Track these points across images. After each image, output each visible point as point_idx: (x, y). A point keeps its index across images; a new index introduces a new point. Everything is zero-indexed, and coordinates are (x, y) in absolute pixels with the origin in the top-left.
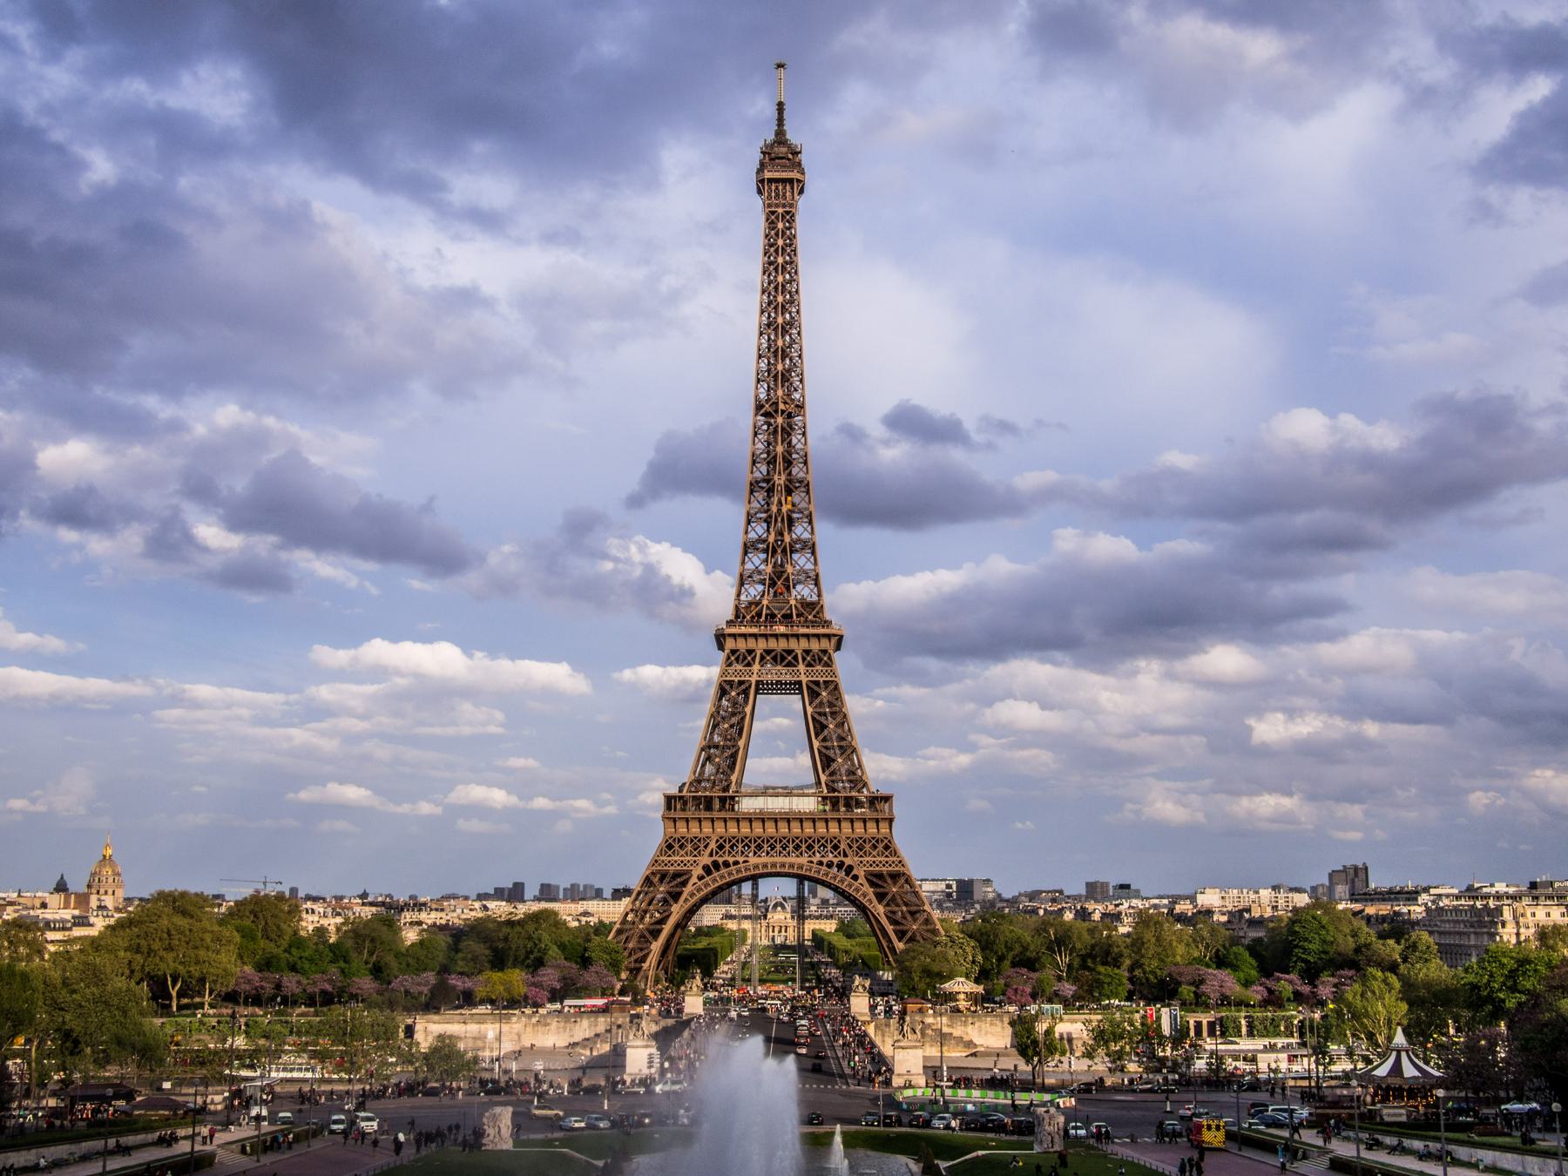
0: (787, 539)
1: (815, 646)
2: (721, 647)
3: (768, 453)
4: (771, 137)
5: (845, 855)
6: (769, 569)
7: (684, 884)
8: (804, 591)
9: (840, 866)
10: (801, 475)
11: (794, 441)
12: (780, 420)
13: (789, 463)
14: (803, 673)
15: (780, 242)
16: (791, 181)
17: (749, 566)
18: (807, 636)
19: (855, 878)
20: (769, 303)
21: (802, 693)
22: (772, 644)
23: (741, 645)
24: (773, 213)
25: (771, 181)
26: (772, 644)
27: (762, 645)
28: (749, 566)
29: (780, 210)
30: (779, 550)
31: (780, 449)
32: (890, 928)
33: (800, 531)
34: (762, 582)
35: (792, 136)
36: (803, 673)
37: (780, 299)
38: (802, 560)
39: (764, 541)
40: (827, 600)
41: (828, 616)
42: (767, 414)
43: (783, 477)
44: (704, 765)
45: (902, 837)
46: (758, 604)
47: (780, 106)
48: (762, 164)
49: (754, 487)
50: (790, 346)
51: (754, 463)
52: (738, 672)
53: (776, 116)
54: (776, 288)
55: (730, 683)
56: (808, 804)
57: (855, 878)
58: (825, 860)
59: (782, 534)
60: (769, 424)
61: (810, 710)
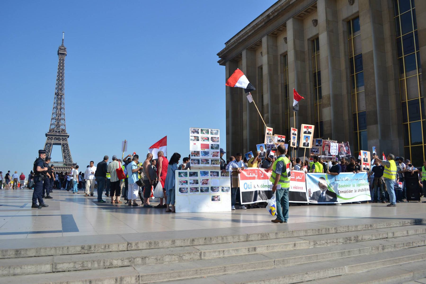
0: (60, 118)
1: (64, 137)
2: (46, 136)
4: (61, 45)
6: (56, 123)
8: (62, 127)
12: (60, 96)
13: (61, 104)
14: (61, 142)
16: (64, 54)
18: (63, 136)
23: (50, 137)
25: (60, 53)
27: (54, 137)
30: (58, 120)
31: (59, 102)
33: (62, 116)
36: (61, 142)
40: (66, 129)
41: (67, 132)
52: (50, 141)
55: (48, 143)
56: (61, 165)
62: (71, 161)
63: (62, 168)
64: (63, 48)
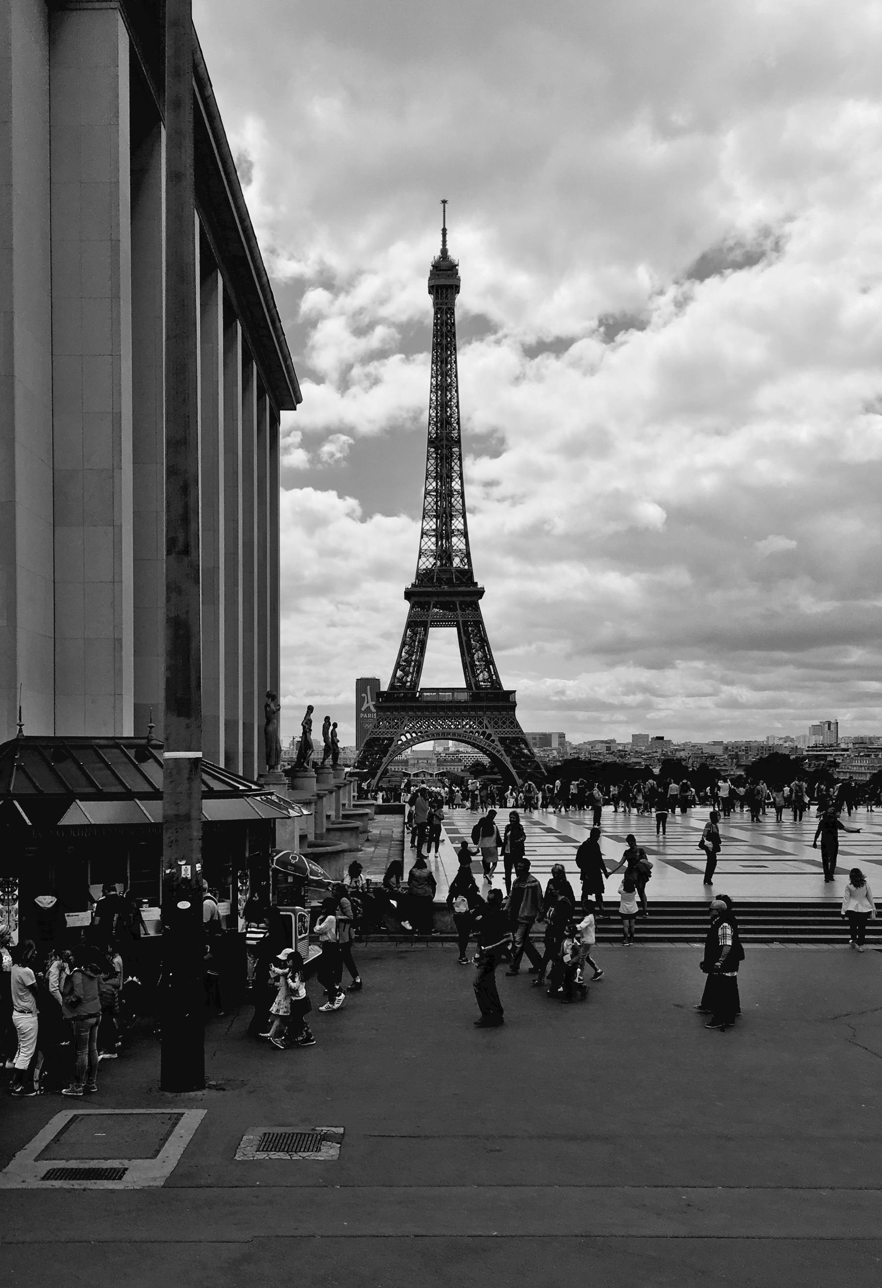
0: (449, 531)
1: (468, 599)
3: (437, 472)
4: (438, 254)
5: (487, 728)
7: (389, 745)
9: (484, 733)
11: (453, 464)
12: (445, 451)
15: (444, 330)
16: (451, 287)
19: (493, 741)
20: (437, 370)
21: (458, 626)
22: (441, 599)
24: (439, 309)
26: (441, 599)
28: (426, 547)
29: (444, 307)
31: (445, 471)
32: (513, 771)
33: (457, 524)
35: (453, 254)
37: (444, 370)
38: (457, 542)
42: (437, 449)
45: (520, 715)
46: (431, 570)
47: (444, 231)
49: (427, 493)
50: (450, 400)
56: (464, 697)
57: (493, 741)
58: (474, 731)
59: (445, 524)
60: (437, 454)
61: (464, 639)
62: (496, 683)
63: (466, 708)
64: (444, 264)
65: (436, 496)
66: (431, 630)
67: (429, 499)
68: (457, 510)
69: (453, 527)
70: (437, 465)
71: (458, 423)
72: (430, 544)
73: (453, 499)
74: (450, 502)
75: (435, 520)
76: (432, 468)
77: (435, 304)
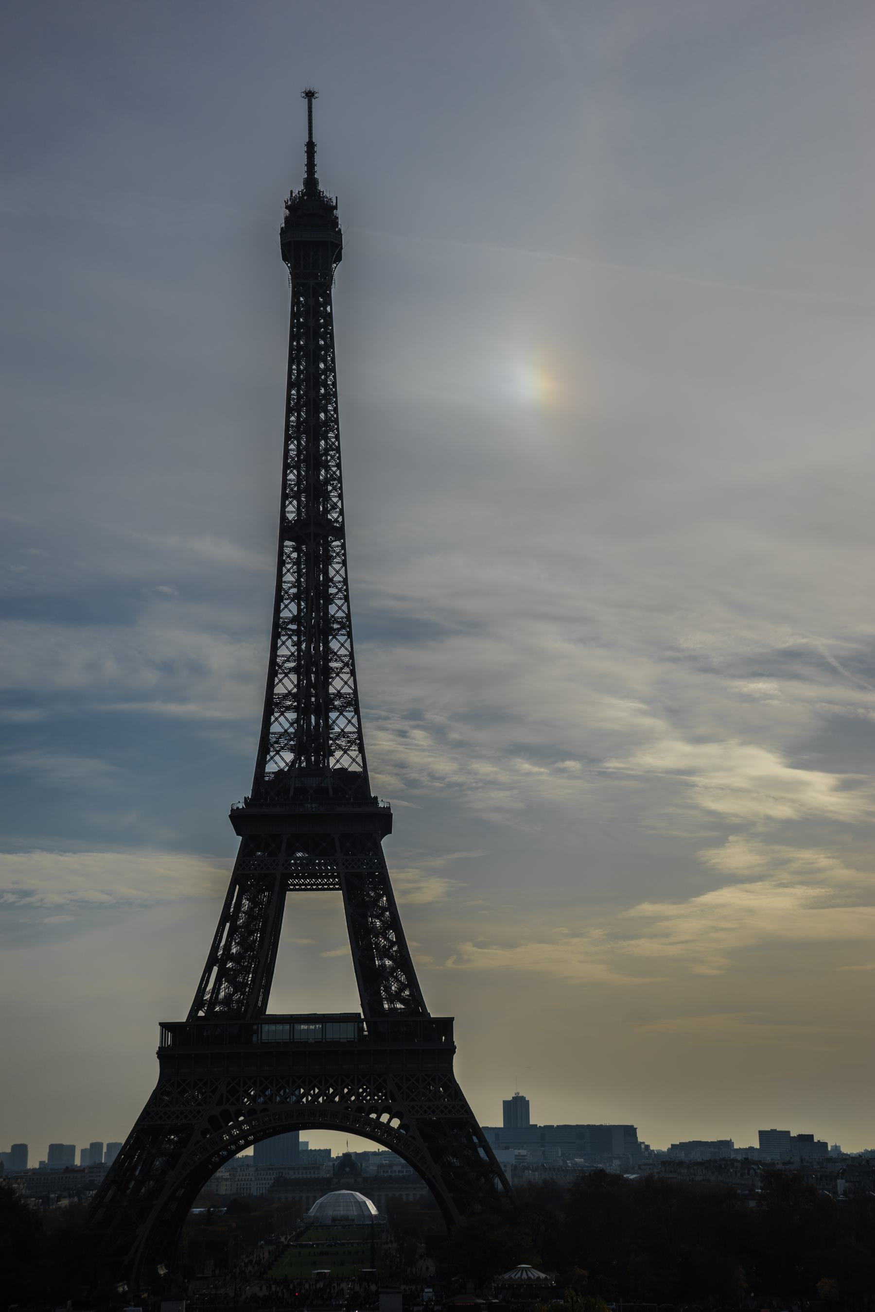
10: (340, 614)
11: (332, 573)
17: (275, 728)
33: (337, 685)
34: (292, 750)
38: (341, 723)
39: (295, 697)
43: (318, 617)
44: (218, 981)
48: (287, 220)
50: (326, 454)
51: (279, 599)
53: (304, 157)
54: (306, 379)
56: (347, 1033)
60: (296, 549)
65: (297, 632)
66: (292, 898)
67: (284, 638)
68: (339, 658)
69: (332, 690)
70: (299, 571)
71: (340, 496)
72: (284, 722)
73: (330, 637)
74: (326, 643)
75: (294, 677)
76: (289, 578)
77: (296, 277)
